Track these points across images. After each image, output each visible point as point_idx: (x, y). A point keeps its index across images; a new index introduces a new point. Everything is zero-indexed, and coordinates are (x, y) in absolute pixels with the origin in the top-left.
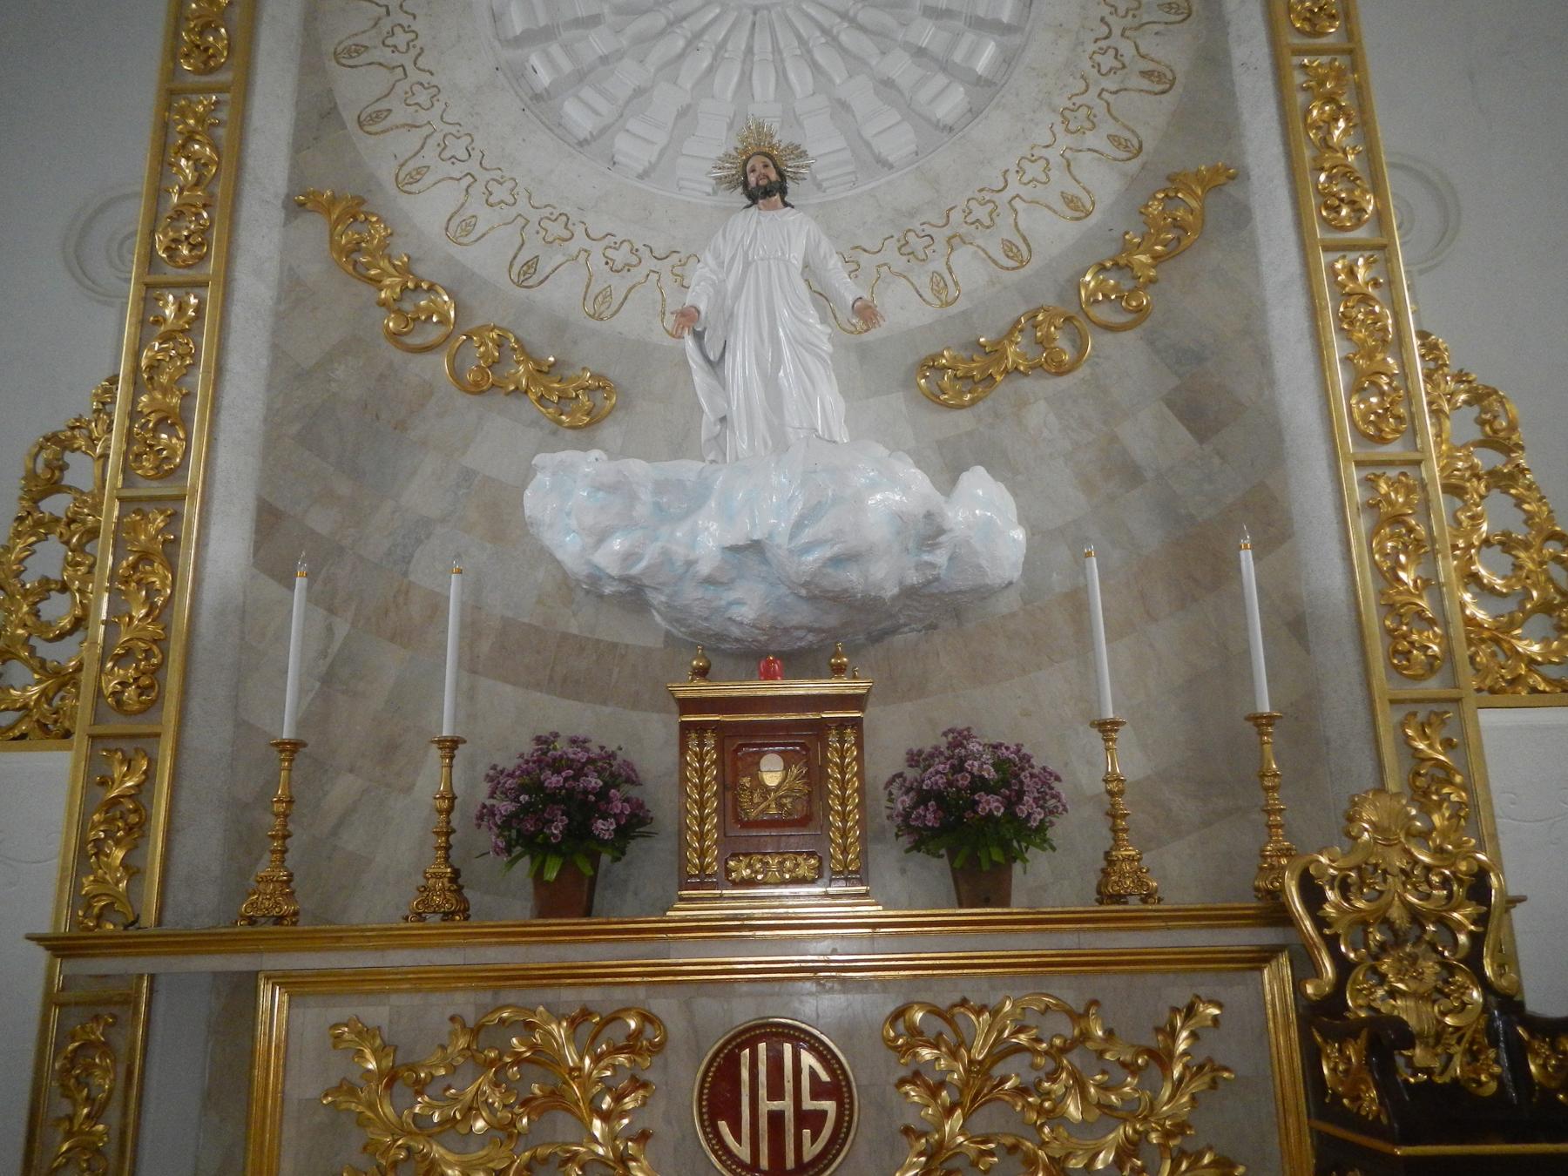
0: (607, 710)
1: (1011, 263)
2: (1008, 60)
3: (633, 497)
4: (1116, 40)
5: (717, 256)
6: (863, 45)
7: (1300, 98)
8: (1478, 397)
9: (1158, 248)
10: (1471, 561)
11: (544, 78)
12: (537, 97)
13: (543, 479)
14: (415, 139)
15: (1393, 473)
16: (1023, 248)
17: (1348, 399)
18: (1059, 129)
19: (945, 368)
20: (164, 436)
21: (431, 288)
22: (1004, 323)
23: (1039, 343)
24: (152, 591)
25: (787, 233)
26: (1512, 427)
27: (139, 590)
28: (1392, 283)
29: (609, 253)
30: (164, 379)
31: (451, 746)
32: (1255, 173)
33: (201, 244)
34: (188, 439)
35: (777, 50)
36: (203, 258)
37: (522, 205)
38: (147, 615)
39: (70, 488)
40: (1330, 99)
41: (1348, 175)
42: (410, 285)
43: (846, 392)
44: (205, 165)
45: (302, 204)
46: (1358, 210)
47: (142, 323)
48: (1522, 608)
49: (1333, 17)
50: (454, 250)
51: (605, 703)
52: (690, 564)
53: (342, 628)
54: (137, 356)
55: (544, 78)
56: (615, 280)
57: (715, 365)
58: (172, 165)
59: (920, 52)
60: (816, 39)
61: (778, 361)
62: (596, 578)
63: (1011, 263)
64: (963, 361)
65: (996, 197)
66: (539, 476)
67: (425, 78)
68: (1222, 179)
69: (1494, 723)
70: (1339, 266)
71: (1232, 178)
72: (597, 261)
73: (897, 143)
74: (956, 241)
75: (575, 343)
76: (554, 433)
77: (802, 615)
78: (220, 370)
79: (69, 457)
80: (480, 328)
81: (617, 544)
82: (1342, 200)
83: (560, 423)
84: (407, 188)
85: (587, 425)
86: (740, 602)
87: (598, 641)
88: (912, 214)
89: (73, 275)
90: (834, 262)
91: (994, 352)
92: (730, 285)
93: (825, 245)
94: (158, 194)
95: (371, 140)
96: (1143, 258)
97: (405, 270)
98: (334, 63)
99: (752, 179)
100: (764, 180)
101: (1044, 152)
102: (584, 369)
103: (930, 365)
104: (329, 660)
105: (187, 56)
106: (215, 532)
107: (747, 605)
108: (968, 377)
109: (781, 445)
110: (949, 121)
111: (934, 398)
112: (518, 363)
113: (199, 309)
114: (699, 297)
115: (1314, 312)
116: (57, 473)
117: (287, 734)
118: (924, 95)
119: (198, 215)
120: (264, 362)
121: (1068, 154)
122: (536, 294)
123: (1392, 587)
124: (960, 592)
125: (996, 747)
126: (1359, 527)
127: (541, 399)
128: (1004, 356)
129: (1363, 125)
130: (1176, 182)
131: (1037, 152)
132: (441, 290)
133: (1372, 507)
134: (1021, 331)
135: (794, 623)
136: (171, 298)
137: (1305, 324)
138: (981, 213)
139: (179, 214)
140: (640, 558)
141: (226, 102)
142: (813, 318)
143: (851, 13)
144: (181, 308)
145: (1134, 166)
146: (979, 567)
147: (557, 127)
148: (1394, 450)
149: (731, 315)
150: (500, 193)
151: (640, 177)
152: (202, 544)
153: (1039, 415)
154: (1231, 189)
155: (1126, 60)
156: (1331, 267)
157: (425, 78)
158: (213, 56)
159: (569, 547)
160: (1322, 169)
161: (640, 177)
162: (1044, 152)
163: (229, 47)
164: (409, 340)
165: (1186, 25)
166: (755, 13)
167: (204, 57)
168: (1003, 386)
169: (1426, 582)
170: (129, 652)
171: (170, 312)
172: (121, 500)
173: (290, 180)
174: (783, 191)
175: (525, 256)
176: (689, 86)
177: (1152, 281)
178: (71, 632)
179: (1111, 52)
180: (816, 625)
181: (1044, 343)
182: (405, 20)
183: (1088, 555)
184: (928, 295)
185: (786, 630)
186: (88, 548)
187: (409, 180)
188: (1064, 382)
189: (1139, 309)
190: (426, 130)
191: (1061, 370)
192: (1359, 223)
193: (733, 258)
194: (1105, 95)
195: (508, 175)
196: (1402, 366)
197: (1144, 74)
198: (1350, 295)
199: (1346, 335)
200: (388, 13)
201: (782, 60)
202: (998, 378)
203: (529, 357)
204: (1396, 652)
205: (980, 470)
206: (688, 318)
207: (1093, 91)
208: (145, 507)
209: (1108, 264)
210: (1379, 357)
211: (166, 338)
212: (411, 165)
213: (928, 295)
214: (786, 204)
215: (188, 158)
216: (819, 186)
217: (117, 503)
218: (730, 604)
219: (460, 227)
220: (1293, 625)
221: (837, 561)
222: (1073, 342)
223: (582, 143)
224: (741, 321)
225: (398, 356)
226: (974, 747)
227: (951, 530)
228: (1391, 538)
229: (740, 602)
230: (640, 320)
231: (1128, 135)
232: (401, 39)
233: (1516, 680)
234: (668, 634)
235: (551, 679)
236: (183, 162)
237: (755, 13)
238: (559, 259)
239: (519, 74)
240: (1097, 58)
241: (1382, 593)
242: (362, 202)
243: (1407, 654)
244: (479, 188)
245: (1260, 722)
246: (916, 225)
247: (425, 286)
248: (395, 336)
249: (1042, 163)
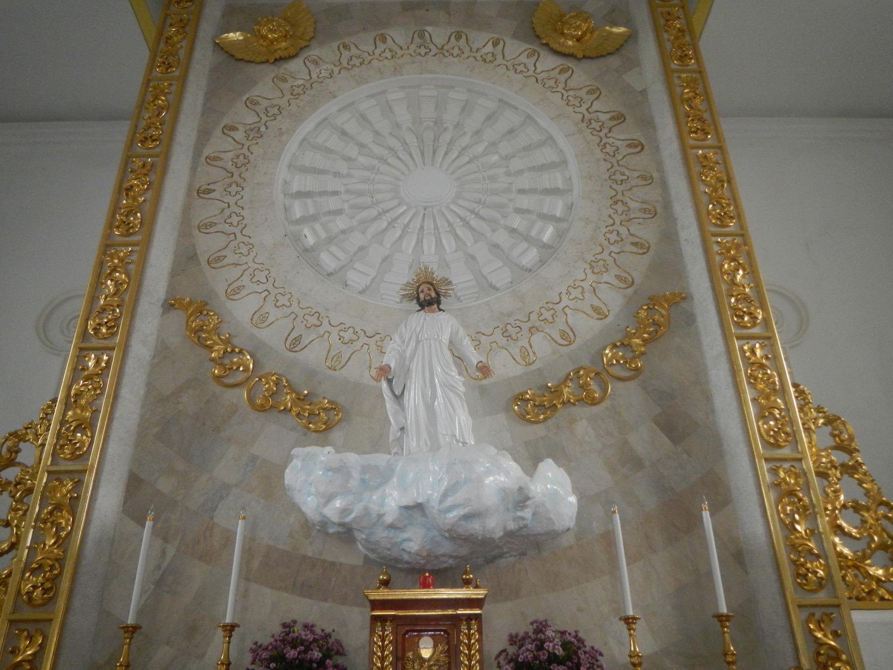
0: (327, 605)
1: (565, 343)
2: (560, 235)
3: (349, 475)
4: (617, 227)
5: (401, 337)
6: (484, 227)
7: (718, 258)
8: (830, 421)
9: (645, 335)
10: (836, 518)
11: (311, 240)
12: (306, 250)
13: (296, 463)
14: (238, 271)
15: (786, 465)
16: (571, 334)
17: (757, 422)
18: (589, 271)
19: (528, 400)
20: (79, 435)
21: (241, 352)
22: (561, 375)
23: (582, 387)
24: (59, 528)
25: (442, 325)
26: (851, 438)
27: (52, 528)
28: (776, 358)
29: (342, 333)
30: (83, 402)
31: (230, 629)
32: (696, 296)
33: (114, 326)
34: (92, 437)
35: (436, 228)
36: (113, 335)
37: (295, 308)
38: (55, 543)
39: (19, 464)
40: (734, 259)
41: (746, 299)
42: (229, 350)
43: (472, 413)
44: (121, 284)
45: (172, 305)
46: (754, 318)
47: (75, 370)
48: (869, 547)
49: (731, 218)
50: (255, 331)
51: (326, 600)
52: (380, 516)
53: (171, 551)
54: (69, 388)
55: (311, 240)
56: (344, 348)
57: (399, 398)
58: (102, 284)
59: (513, 231)
60: (457, 223)
61: (434, 396)
62: (325, 523)
63: (565, 343)
64: (539, 396)
65: (556, 307)
66: (295, 461)
67: (246, 240)
68: (679, 299)
69: (861, 619)
70: (746, 348)
71: (684, 299)
72: (334, 338)
73: (501, 276)
74: (533, 330)
75: (320, 383)
76: (305, 434)
77: (446, 548)
78: (116, 397)
79: (22, 445)
80: (267, 374)
81: (338, 503)
82: (744, 312)
83: (309, 428)
84: (231, 297)
85: (324, 430)
86: (409, 540)
87: (324, 561)
88: (509, 315)
89: (40, 338)
90: (467, 341)
91: (556, 392)
92: (408, 353)
93: (462, 332)
94: (93, 299)
95: (214, 271)
96: (637, 341)
97: (227, 342)
98: (197, 231)
99: (422, 296)
100: (428, 296)
101: (581, 284)
102: (324, 398)
103: (520, 398)
104: (161, 572)
105: (118, 227)
106: (102, 491)
107: (414, 542)
108: (542, 405)
109: (435, 446)
110: (529, 266)
111: (522, 417)
112: (287, 394)
113: (108, 362)
114: (390, 360)
115: (734, 373)
116: (13, 455)
117: (130, 621)
118: (515, 253)
119: (114, 311)
120: (142, 392)
121: (594, 285)
122: (300, 356)
123: (793, 534)
124: (539, 534)
125: (563, 633)
126: (769, 498)
127: (298, 415)
128: (562, 394)
129: (752, 272)
130: (653, 302)
131: (578, 283)
132: (246, 353)
133: (776, 485)
134: (571, 380)
135: (440, 553)
136: (93, 356)
137: (730, 379)
138: (547, 315)
139: (103, 310)
140: (351, 512)
141: (136, 252)
142: (454, 372)
143: (476, 210)
144: (98, 362)
145: (630, 291)
146: (550, 519)
147: (316, 266)
148: (786, 452)
149: (408, 370)
150: (283, 300)
151: (360, 293)
152: (93, 499)
153: (582, 427)
154: (684, 305)
155: (624, 237)
156: (741, 348)
157: (246, 240)
158: (132, 227)
159: (309, 504)
160: (732, 296)
161: (360, 293)
162: (581, 284)
163: (141, 223)
164: (226, 381)
165: (653, 220)
166: (425, 209)
167: (127, 228)
168: (562, 411)
169: (812, 531)
170: (41, 566)
171: (91, 364)
172: (49, 472)
173: (167, 292)
174: (439, 303)
175: (294, 335)
176: (388, 246)
177: (643, 354)
178: (7, 552)
179: (615, 233)
180: (454, 554)
181: (584, 387)
182: (238, 210)
183: (614, 512)
184: (519, 359)
185: (436, 557)
186: (25, 500)
187: (233, 293)
188: (595, 409)
189: (637, 369)
190: (245, 267)
191: (594, 402)
192: (754, 325)
193: (411, 338)
194: (613, 254)
195: (287, 291)
196: (786, 403)
197: (633, 244)
198: (753, 364)
199: (753, 386)
200: (229, 206)
201: (439, 233)
202: (559, 406)
203: (293, 390)
204: (798, 575)
205: (550, 461)
206: (384, 372)
207: (606, 253)
208: (61, 476)
209: (618, 344)
210: (773, 398)
211: (87, 378)
212: (235, 285)
213: (519, 359)
214: (440, 310)
215: (112, 280)
216: (458, 299)
217: (46, 474)
218: (404, 540)
219: (260, 318)
220: (736, 556)
221: (467, 517)
222: (600, 386)
223: (330, 275)
224: (414, 373)
225: (218, 389)
226: (550, 633)
227: (534, 497)
228: (789, 504)
229: (409, 540)
230: (357, 371)
231: (626, 275)
232: (235, 219)
233: (870, 593)
234: (366, 557)
235: (294, 585)
236: (109, 282)
237: (425, 209)
238: (313, 336)
239: (297, 239)
240: (608, 235)
241: (787, 538)
242: (207, 304)
243: (805, 576)
244: (271, 298)
245: (720, 618)
246: (511, 321)
247: (237, 350)
248: (218, 378)
249: (580, 289)
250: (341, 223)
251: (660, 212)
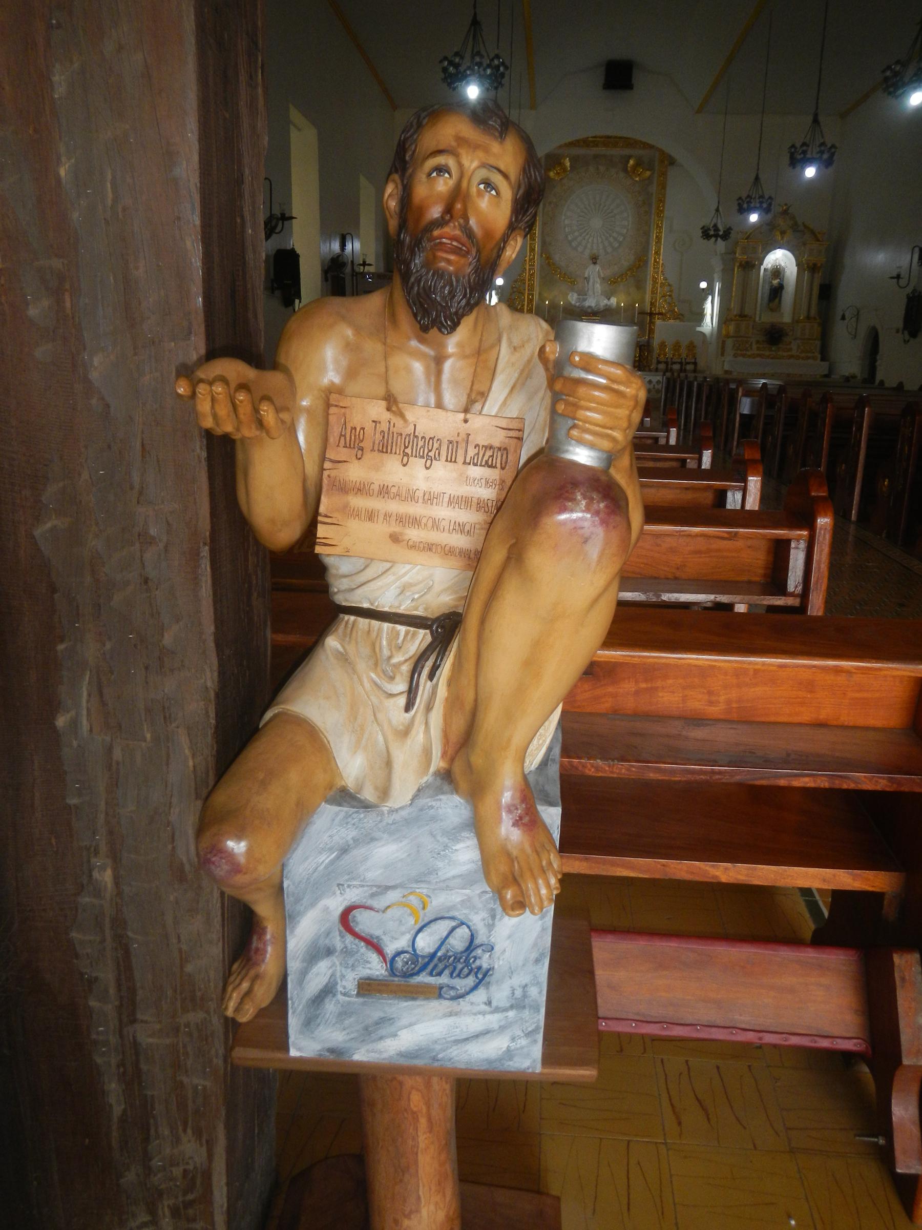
25: (598, 268)
100: (594, 260)
107: (589, 310)
114: (586, 275)
159: (573, 303)
250: (576, 234)
251: (647, 234)
